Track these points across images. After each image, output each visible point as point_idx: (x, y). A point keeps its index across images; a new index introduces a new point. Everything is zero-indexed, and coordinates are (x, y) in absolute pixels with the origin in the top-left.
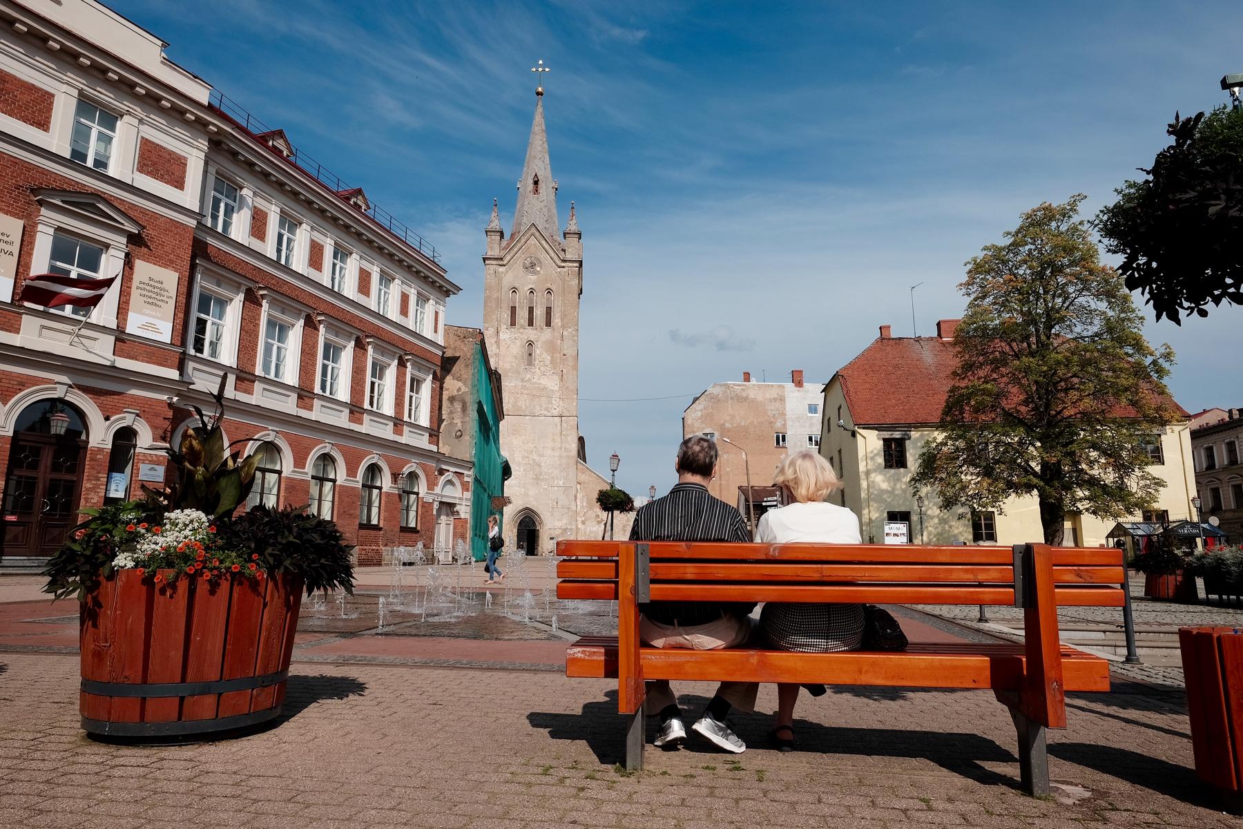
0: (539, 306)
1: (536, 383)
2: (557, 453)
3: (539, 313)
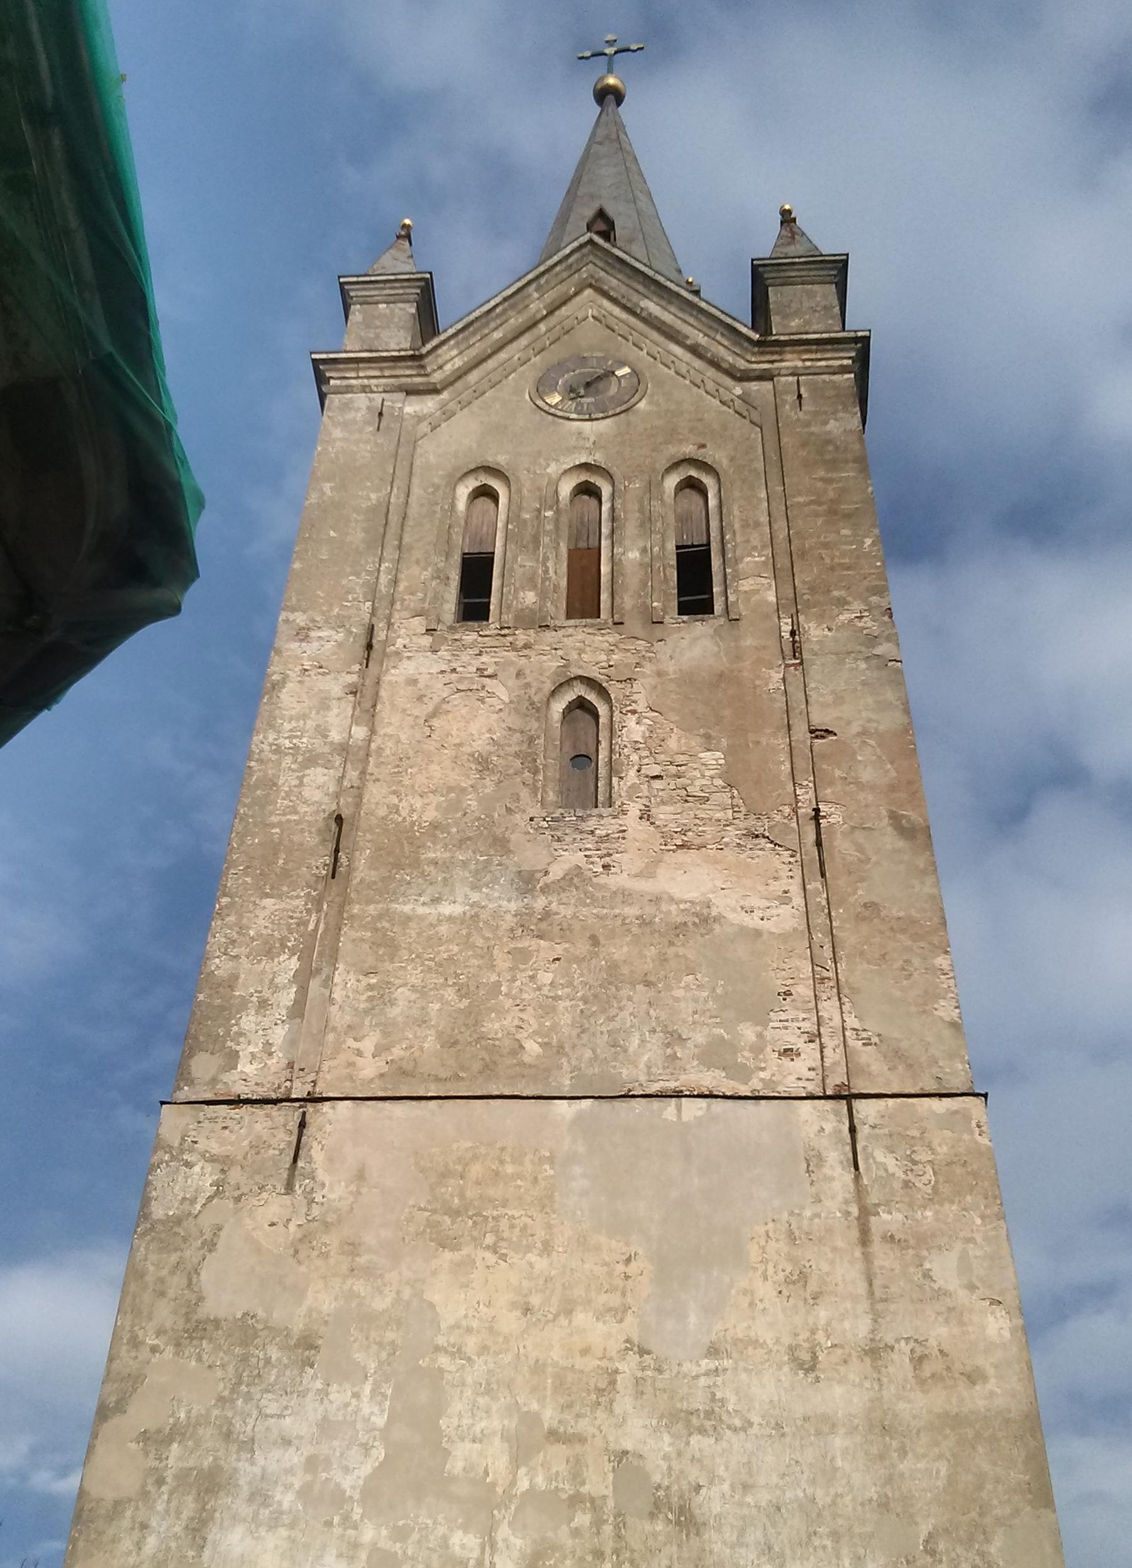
1: (626, 896)
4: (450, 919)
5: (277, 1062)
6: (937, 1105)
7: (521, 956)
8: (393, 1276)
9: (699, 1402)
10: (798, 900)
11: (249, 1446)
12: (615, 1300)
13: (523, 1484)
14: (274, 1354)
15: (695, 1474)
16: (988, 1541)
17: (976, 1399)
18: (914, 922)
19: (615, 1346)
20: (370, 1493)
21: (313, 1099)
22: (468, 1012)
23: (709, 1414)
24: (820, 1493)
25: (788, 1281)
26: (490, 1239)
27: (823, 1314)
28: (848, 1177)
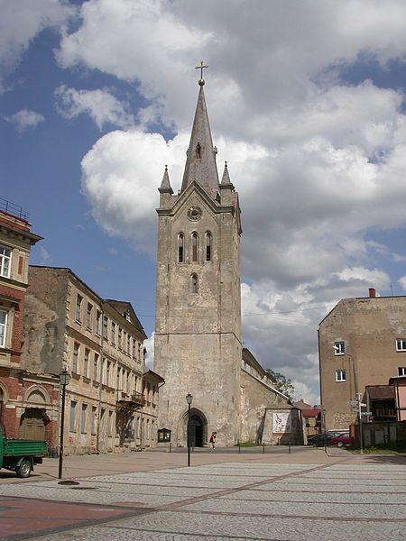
0: (200, 245)
2: (217, 363)
3: (202, 250)
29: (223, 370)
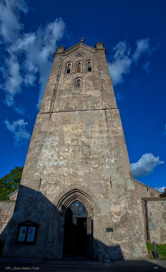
1: (83, 94)
4: (66, 97)
5: (48, 110)
6: (114, 110)
7: (73, 100)
8: (59, 127)
9: (90, 136)
10: (100, 94)
11: (45, 142)
12: (82, 128)
13: (72, 144)
14: (48, 134)
15: (90, 142)
16: (119, 147)
17: (118, 135)
18: (112, 95)
19: (82, 132)
20: (57, 146)
21: (52, 112)
22: (67, 105)
23: (91, 137)
24: (102, 144)
25: (99, 125)
26: (69, 123)
27: (103, 128)
28: (105, 116)
29: (113, 141)
